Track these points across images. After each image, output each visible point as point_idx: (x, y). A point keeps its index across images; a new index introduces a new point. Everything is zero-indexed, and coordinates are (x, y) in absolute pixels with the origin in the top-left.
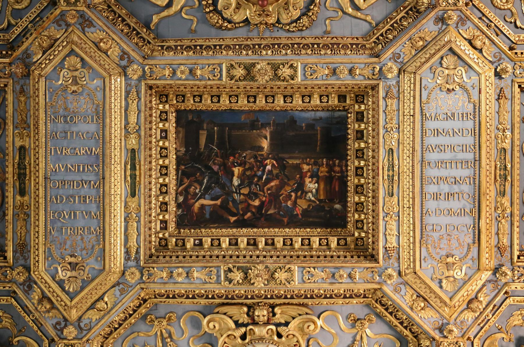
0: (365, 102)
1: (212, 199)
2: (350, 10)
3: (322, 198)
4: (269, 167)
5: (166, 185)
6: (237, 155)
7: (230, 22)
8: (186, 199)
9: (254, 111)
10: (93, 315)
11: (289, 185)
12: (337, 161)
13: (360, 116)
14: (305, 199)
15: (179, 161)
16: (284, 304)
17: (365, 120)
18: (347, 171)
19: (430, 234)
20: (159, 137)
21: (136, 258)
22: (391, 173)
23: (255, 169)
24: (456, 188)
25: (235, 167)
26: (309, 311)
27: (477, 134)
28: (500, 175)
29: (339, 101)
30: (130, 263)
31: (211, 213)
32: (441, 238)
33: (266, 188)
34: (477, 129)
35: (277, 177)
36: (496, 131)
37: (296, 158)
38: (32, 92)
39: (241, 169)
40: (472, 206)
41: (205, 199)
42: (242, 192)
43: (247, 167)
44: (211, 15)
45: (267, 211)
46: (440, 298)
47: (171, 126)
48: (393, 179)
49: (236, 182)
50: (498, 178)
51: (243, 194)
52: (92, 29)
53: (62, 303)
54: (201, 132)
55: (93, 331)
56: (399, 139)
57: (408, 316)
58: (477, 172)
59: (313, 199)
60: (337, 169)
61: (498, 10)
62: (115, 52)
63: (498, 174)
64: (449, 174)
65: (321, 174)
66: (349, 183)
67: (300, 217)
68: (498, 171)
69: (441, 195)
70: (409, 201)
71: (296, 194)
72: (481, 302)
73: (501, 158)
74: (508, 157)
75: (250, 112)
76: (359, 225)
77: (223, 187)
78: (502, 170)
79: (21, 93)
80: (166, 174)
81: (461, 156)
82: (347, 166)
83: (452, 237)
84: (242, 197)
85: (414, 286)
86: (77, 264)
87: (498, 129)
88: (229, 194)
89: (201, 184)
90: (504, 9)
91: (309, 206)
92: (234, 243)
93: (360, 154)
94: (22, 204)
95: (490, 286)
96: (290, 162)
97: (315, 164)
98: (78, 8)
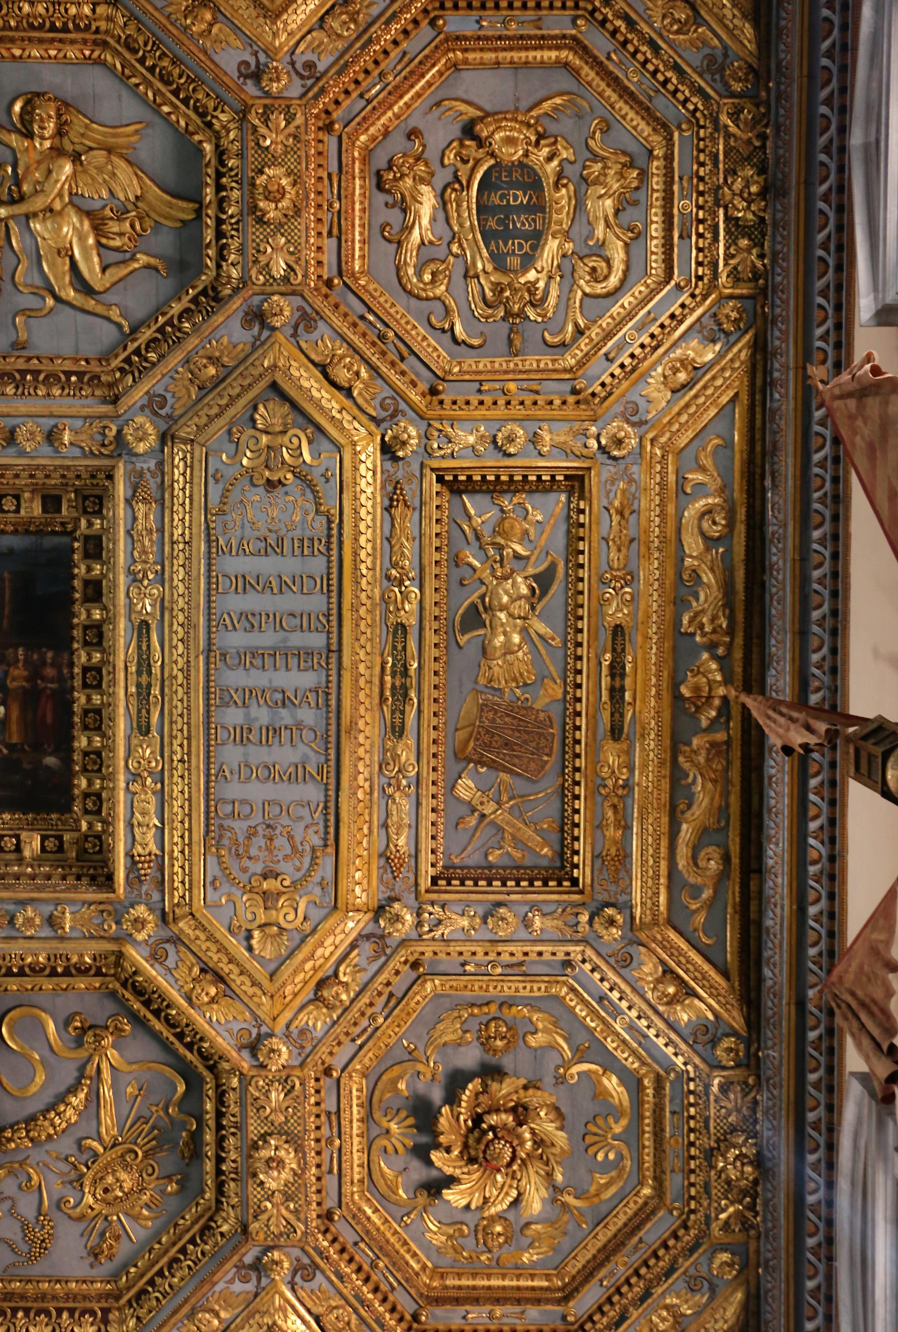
2: (70, 294)
19: (226, 823)
22: (144, 679)
24: (285, 716)
27: (334, 588)
28: (393, 687)
29: (45, 510)
32: (252, 833)
34: (334, 576)
36: (385, 583)
40: (322, 759)
48: (149, 694)
50: (388, 693)
56: (163, 600)
58: (334, 678)
61: (414, 302)
63: (389, 685)
64: (270, 681)
68: (388, 678)
69: (250, 730)
70: (181, 746)
73: (394, 648)
74: (412, 645)
78: (398, 676)
81: (297, 640)
83: (278, 832)
87: (388, 578)
90: (428, 299)
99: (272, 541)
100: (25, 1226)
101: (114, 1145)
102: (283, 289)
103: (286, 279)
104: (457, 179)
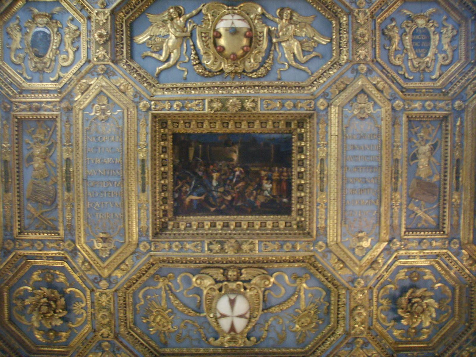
0: (305, 127)
1: (198, 195)
2: (294, 64)
3: (274, 194)
4: (237, 173)
5: (166, 185)
6: (215, 165)
7: (210, 71)
8: (180, 195)
9: (228, 134)
10: (118, 274)
11: (251, 185)
12: (285, 169)
13: (301, 137)
14: (263, 195)
15: (175, 169)
16: (248, 267)
17: (304, 139)
18: (292, 175)
20: (161, 152)
21: (146, 235)
23: (228, 174)
25: (214, 172)
26: (265, 272)
30: (143, 239)
31: (198, 206)
33: (235, 188)
35: (243, 179)
37: (256, 167)
38: (74, 121)
39: (218, 174)
41: (193, 195)
42: (219, 190)
43: (222, 172)
44: (197, 66)
45: (236, 203)
46: (353, 261)
47: (169, 144)
49: (215, 183)
51: (220, 192)
52: (115, 77)
53: (98, 265)
54: (190, 148)
55: (119, 284)
57: (332, 274)
59: (268, 195)
60: (285, 174)
62: (130, 93)
65: (274, 178)
66: (293, 184)
67: (259, 208)
71: (257, 191)
72: (379, 263)
75: (224, 134)
76: (300, 213)
77: (205, 187)
79: (67, 122)
80: (166, 178)
82: (292, 172)
84: (219, 194)
85: (336, 253)
86: (106, 238)
88: (210, 191)
89: (190, 185)
91: (265, 200)
92: (213, 225)
93: (301, 163)
94: (69, 198)
95: (386, 252)
96: (253, 169)
97: (270, 170)
98: (106, 63)
99: (361, 135)
100: (278, 334)
101: (305, 310)
102: (364, 62)
103: (364, 59)
104: (405, 31)
